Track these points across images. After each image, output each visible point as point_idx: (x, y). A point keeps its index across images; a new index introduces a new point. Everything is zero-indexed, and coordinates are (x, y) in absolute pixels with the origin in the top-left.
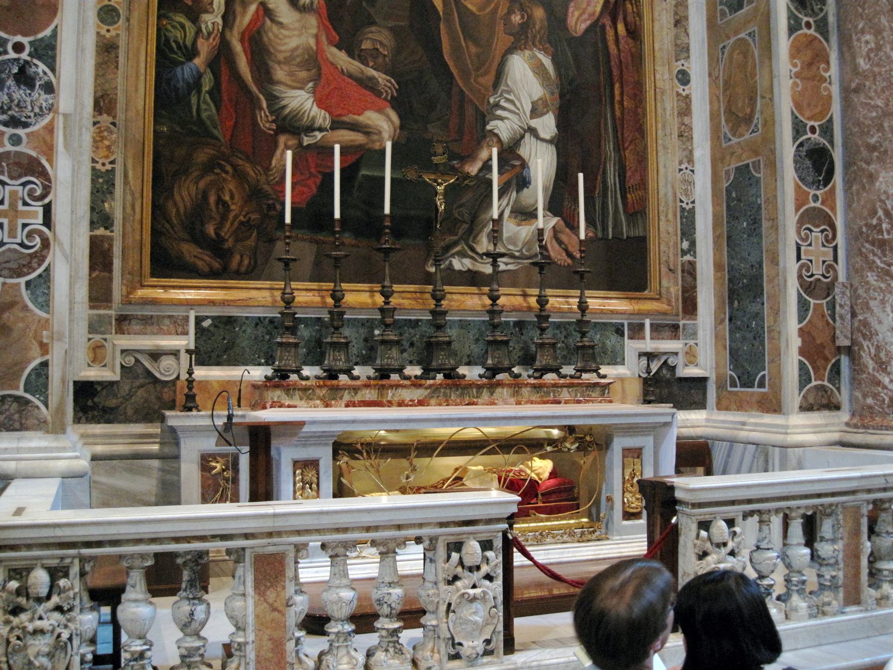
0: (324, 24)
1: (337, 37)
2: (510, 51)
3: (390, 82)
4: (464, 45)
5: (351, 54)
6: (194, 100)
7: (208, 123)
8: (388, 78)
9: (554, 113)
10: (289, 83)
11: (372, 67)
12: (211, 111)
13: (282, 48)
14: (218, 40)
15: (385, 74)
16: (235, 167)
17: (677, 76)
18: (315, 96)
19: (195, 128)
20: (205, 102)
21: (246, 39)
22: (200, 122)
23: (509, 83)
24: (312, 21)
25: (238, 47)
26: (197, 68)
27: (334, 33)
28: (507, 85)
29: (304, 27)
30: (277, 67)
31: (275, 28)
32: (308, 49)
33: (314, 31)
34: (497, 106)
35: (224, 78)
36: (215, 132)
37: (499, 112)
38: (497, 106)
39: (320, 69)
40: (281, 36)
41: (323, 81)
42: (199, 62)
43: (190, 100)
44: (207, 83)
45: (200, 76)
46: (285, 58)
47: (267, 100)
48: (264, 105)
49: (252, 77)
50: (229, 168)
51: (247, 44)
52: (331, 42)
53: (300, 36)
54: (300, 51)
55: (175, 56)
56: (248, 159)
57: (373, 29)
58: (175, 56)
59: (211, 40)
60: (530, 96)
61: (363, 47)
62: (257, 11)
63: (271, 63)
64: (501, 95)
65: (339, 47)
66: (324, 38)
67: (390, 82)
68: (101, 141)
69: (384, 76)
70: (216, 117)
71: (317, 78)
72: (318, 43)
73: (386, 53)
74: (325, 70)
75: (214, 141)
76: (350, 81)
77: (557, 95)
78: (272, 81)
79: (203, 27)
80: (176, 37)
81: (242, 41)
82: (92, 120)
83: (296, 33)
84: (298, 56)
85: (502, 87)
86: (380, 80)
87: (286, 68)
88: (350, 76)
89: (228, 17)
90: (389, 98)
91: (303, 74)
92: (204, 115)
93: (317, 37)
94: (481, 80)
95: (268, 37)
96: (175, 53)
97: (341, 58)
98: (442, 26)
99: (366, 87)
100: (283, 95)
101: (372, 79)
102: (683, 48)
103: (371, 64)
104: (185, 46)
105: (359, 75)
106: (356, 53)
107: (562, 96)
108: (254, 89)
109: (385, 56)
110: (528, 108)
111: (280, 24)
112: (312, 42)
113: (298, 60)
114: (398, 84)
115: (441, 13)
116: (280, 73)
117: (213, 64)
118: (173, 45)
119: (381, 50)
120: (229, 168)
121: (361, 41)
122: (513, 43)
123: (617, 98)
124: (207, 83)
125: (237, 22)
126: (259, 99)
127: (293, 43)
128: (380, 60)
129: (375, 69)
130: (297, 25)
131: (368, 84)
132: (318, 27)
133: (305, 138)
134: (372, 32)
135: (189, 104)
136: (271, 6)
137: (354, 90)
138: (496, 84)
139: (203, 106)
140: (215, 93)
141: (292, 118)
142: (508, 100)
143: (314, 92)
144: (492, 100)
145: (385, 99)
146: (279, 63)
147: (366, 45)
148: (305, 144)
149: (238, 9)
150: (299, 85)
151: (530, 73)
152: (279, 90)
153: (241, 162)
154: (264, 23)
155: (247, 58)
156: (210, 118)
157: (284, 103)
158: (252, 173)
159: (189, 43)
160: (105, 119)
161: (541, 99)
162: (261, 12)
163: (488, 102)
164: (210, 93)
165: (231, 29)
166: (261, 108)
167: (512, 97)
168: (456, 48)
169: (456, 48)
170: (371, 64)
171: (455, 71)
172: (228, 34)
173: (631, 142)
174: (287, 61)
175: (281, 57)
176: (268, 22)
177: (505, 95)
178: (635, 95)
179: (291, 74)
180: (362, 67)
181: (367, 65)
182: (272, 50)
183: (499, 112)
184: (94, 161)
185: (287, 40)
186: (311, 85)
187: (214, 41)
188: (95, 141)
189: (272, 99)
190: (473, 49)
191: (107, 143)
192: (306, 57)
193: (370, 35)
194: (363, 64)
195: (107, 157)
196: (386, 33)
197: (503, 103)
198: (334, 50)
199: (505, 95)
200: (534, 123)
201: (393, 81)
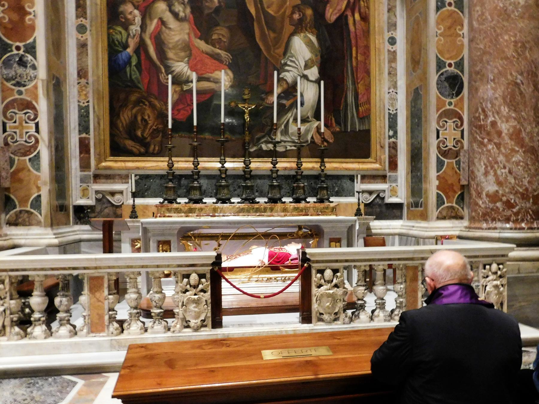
0: (193, 28)
1: (199, 34)
2: (293, 34)
3: (228, 56)
4: (267, 32)
5: (207, 42)
6: (128, 69)
7: (136, 81)
8: (227, 53)
9: (317, 66)
10: (176, 59)
11: (218, 48)
12: (136, 74)
13: (171, 41)
14: (138, 38)
15: (225, 51)
16: (150, 102)
17: (388, 41)
18: (189, 65)
19: (129, 84)
20: (134, 71)
21: (153, 37)
22: (131, 80)
23: (292, 52)
24: (186, 26)
25: (149, 42)
26: (129, 54)
27: (198, 32)
28: (291, 53)
29: (182, 29)
30: (168, 51)
31: (167, 31)
32: (184, 41)
33: (187, 31)
34: (286, 64)
35: (143, 57)
36: (140, 85)
37: (287, 68)
38: (286, 64)
39: (191, 50)
40: (170, 35)
41: (192, 57)
42: (129, 50)
43: (126, 70)
46: (173, 46)
47: (165, 68)
48: (163, 71)
49: (157, 56)
50: (147, 103)
51: (153, 40)
52: (196, 36)
53: (180, 34)
54: (180, 42)
55: (117, 48)
56: (156, 99)
57: (218, 28)
58: (117, 48)
59: (135, 39)
60: (304, 58)
61: (213, 38)
62: (157, 23)
63: (166, 49)
64: (288, 58)
65: (200, 38)
66: (192, 35)
67: (228, 56)
68: (82, 92)
69: (225, 53)
70: (139, 78)
71: (190, 56)
72: (189, 37)
73: (225, 40)
74: (193, 52)
75: (139, 90)
76: (207, 56)
77: (319, 57)
78: (167, 59)
79: (131, 32)
80: (117, 38)
81: (151, 38)
82: (77, 82)
83: (178, 32)
84: (179, 45)
85: (289, 54)
86: (222, 54)
87: (174, 51)
88: (207, 54)
89: (143, 27)
90: (227, 63)
91: (182, 54)
92: (133, 77)
93: (189, 34)
94: (277, 51)
95: (164, 36)
96: (118, 47)
97: (202, 45)
98: (255, 24)
99: (215, 59)
100: (173, 65)
101: (218, 54)
102: (393, 24)
103: (218, 47)
104: (122, 43)
105: (211, 53)
106: (210, 41)
107: (322, 57)
108: (158, 63)
109: (225, 42)
110: (303, 64)
111: (170, 29)
112: (186, 37)
113: (180, 47)
114: (232, 56)
115: (255, 17)
116: (171, 54)
117: (137, 51)
118: (117, 42)
119: (223, 39)
120: (147, 103)
121: (212, 35)
122: (294, 30)
123: (354, 55)
125: (148, 30)
126: (160, 68)
127: (176, 38)
128: (222, 44)
129: (220, 49)
130: (178, 29)
132: (190, 29)
133: (185, 87)
134: (217, 30)
135: (126, 72)
136: (165, 19)
137: (209, 61)
138: (285, 54)
139: (133, 73)
140: (138, 65)
141: (177, 77)
142: (291, 61)
143: (188, 63)
144: (283, 62)
145: (225, 64)
146: (169, 49)
147: (215, 37)
148: (185, 89)
149: (148, 22)
150: (180, 60)
151: (304, 46)
152: (170, 63)
153: (152, 100)
154: (161, 28)
155: (154, 47)
156: (136, 78)
157: (173, 69)
158: (158, 105)
159: (124, 41)
160: (83, 81)
161: (310, 59)
162: (160, 23)
163: (281, 63)
164: (135, 66)
165: (145, 32)
166: (162, 73)
167: (294, 59)
168: (263, 36)
169: (263, 36)
170: (218, 47)
171: (262, 48)
172: (143, 35)
173: (362, 79)
174: (174, 48)
175: (171, 46)
176: (164, 28)
177: (290, 59)
178: (365, 53)
179: (176, 54)
180: (213, 48)
181: (216, 47)
182: (166, 42)
183: (287, 68)
184: (79, 102)
185: (173, 37)
186: (186, 59)
188: (79, 92)
190: (272, 35)
191: (84, 92)
192: (184, 45)
193: (217, 32)
194: (213, 47)
195: (85, 99)
196: (225, 29)
197: (289, 63)
198: (199, 41)
199: (290, 59)
200: (306, 72)
201: (229, 55)
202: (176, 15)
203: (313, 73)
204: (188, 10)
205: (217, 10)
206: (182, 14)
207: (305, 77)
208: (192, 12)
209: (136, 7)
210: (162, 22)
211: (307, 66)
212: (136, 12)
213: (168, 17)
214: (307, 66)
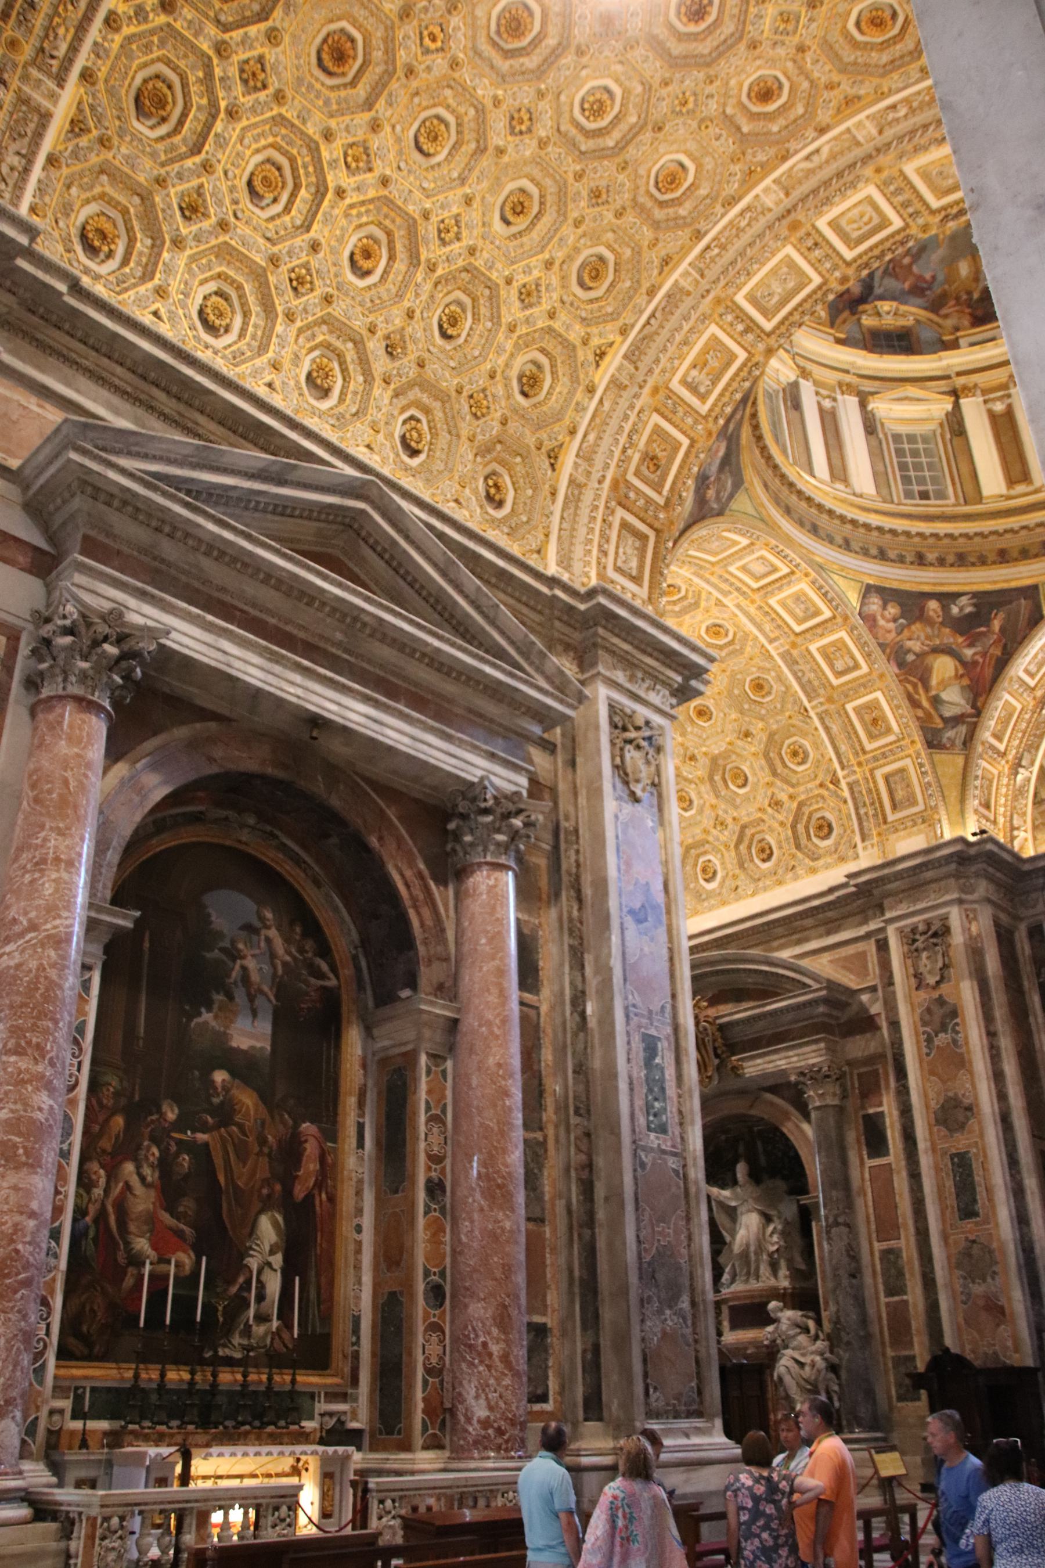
24: (152, 1193)
25: (110, 1209)
44: (92, 1233)
45: (87, 1228)
88: (170, 1229)
89: (107, 1191)
91: (145, 1228)
97: (166, 1218)
110: (267, 1248)
116: (132, 1227)
117: (96, 1221)
124: (92, 1233)
131: (179, 1234)
140: (95, 1240)
147: (181, 1209)
187: (98, 1206)
189: (127, 1243)
202: (142, 1179)
203: (277, 1260)
204: (157, 1174)
205: (186, 1177)
206: (149, 1179)
207: (269, 1265)
208: (161, 1177)
209: (102, 1166)
210: (128, 1187)
211: (272, 1252)
212: (102, 1172)
213: (135, 1181)
214: (272, 1252)
